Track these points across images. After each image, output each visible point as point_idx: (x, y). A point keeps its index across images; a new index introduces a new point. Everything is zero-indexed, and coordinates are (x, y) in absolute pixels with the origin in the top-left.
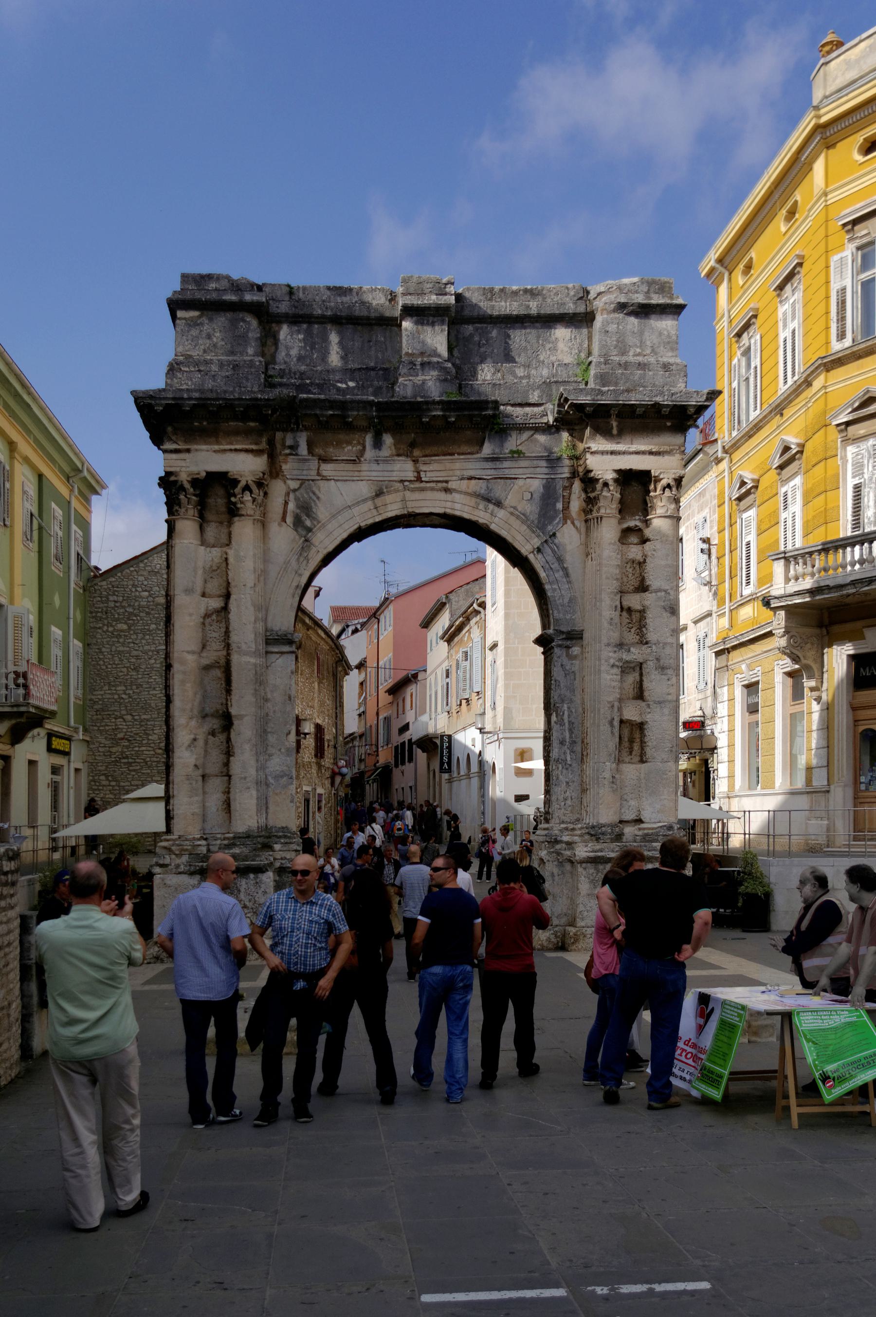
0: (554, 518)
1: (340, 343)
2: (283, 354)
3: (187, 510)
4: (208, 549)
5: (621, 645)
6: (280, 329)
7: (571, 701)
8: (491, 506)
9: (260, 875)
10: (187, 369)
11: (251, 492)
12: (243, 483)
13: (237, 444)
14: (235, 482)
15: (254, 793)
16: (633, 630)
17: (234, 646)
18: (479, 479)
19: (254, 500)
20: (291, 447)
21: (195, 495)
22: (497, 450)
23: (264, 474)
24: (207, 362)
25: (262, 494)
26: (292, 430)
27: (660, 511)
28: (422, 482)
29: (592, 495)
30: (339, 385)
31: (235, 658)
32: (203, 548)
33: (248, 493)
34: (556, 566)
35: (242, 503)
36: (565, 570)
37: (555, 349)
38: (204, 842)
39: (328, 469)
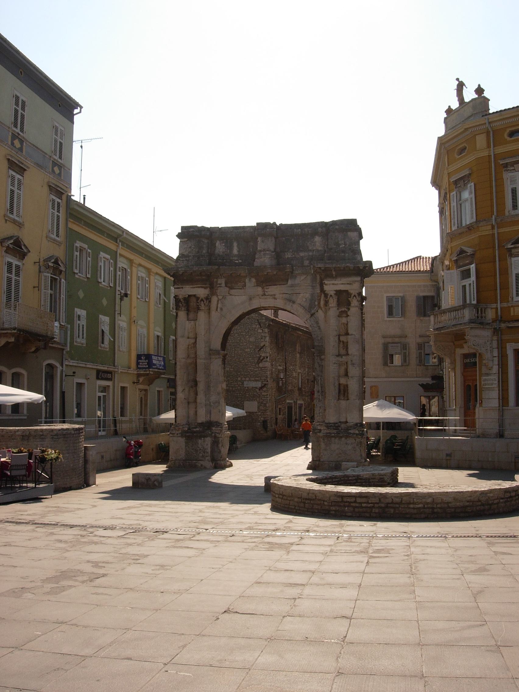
0: (314, 308)
1: (238, 246)
2: (217, 251)
3: (182, 308)
4: (190, 322)
5: (339, 355)
6: (217, 242)
7: (322, 376)
8: (291, 304)
9: (205, 438)
10: (182, 259)
11: (204, 301)
12: (200, 299)
13: (199, 285)
14: (198, 298)
15: (204, 409)
16: (345, 349)
17: (198, 356)
18: (287, 294)
19: (204, 304)
20: (219, 284)
21: (185, 303)
22: (293, 283)
23: (208, 295)
24: (188, 256)
25: (208, 302)
26: (220, 278)
27: (352, 305)
28: (266, 295)
29: (327, 300)
30: (236, 261)
31: (198, 361)
32: (188, 321)
33: (202, 302)
34: (315, 325)
35: (201, 306)
36: (319, 327)
37: (315, 245)
38: (187, 426)
39: (233, 292)
